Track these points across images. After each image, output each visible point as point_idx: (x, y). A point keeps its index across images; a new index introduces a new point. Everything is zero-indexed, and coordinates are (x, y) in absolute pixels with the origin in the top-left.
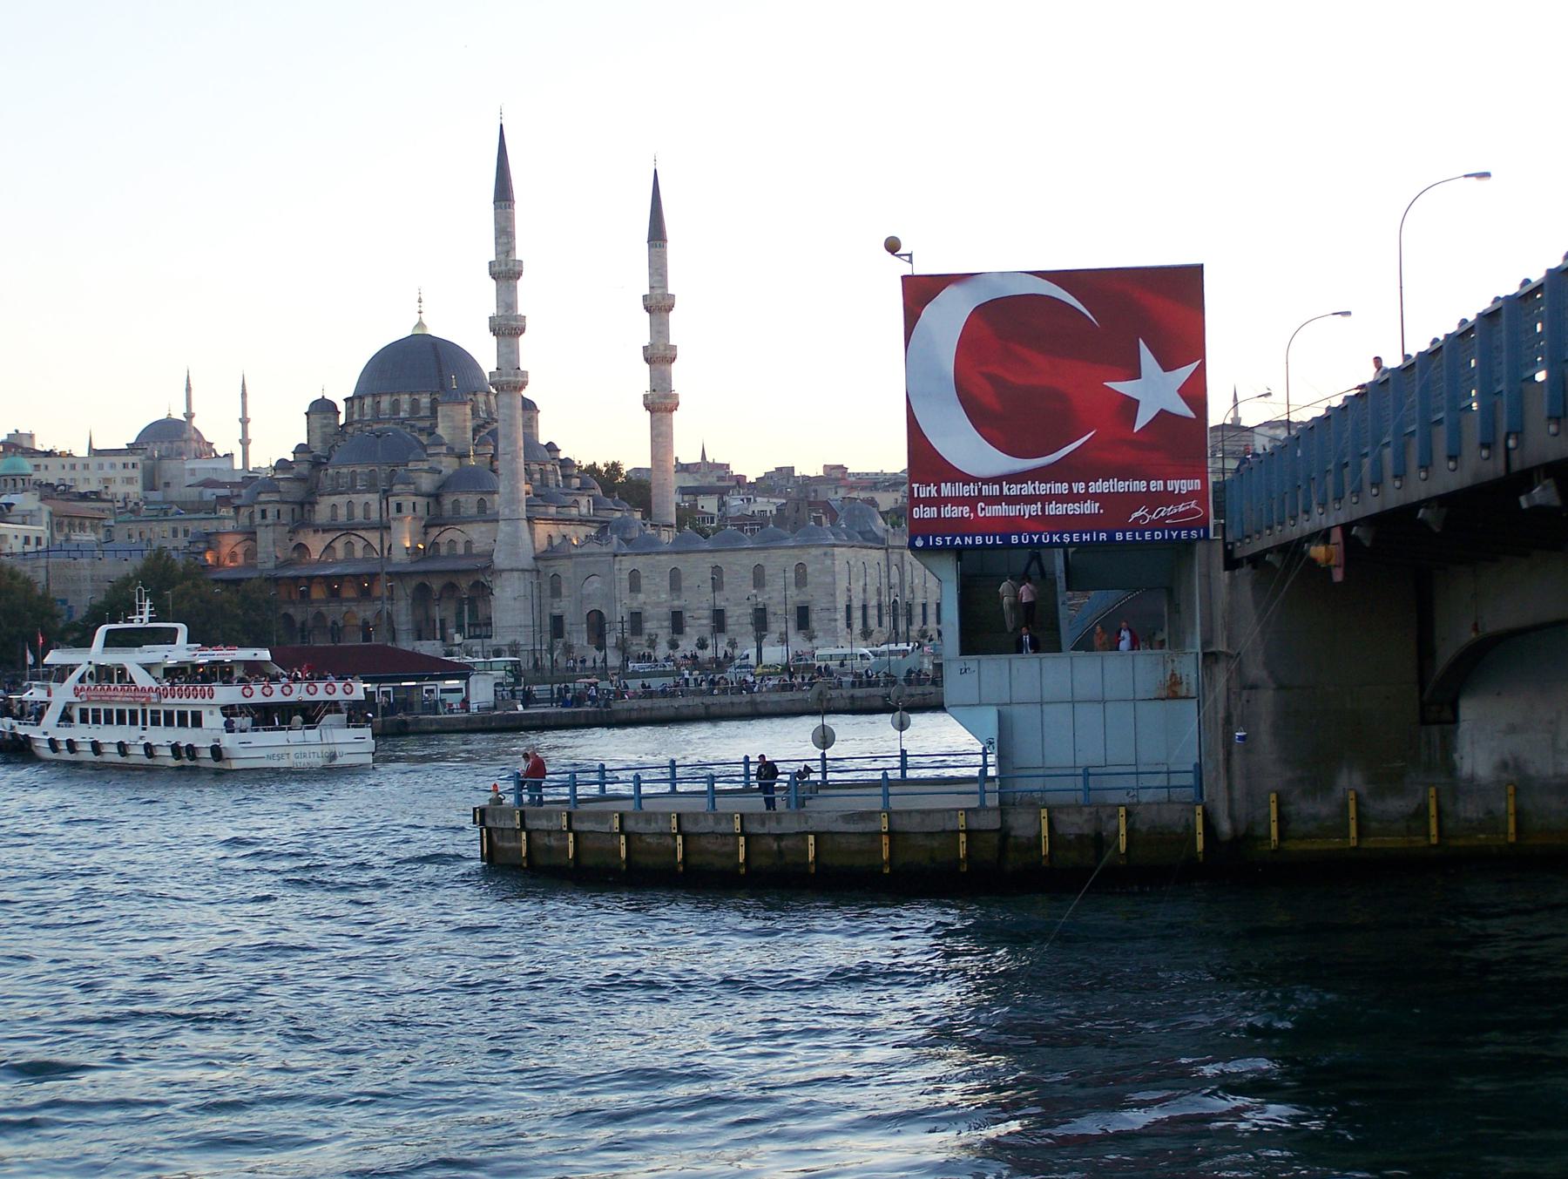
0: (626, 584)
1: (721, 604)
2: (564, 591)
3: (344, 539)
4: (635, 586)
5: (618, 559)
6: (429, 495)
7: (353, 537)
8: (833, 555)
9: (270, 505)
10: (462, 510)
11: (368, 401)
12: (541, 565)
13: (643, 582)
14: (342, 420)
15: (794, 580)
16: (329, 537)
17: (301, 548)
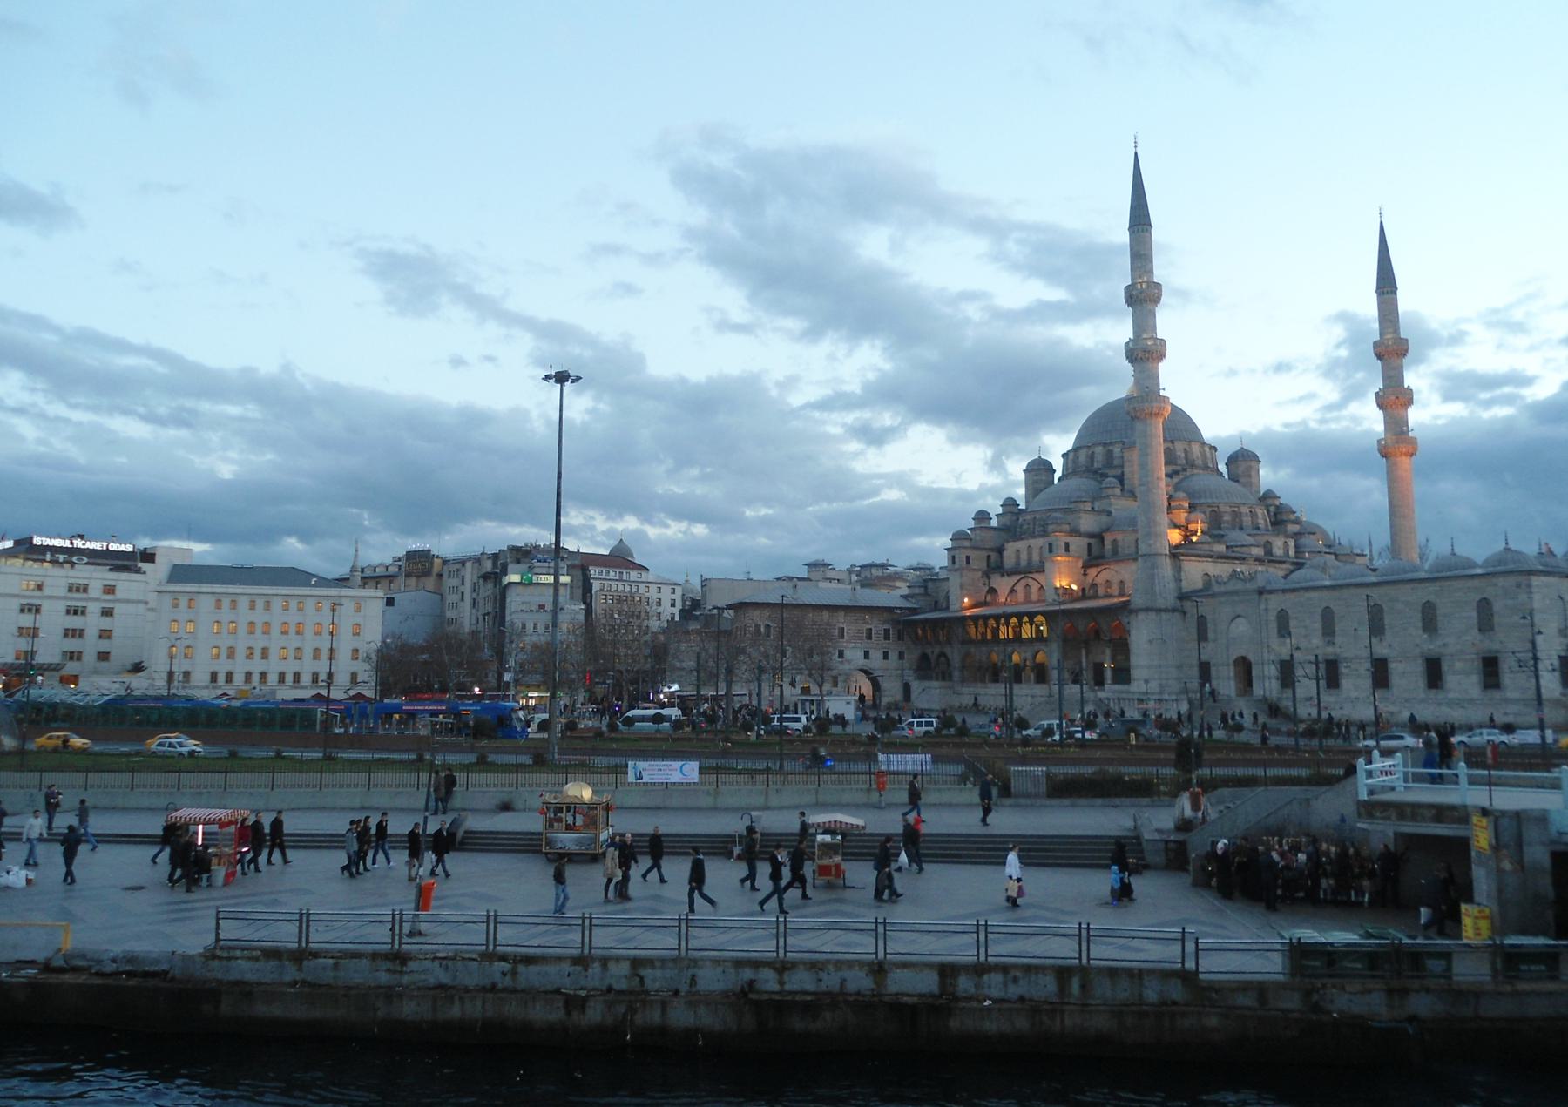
0: (1273, 627)
1: (1381, 650)
2: (1211, 635)
3: (1023, 581)
4: (1284, 630)
5: (1265, 596)
6: (1090, 535)
7: (1030, 580)
8: (1529, 586)
9: (958, 552)
10: (1120, 550)
11: (1071, 456)
12: (1188, 605)
13: (1292, 623)
14: (1058, 475)
15: (1475, 621)
16: (1016, 578)
17: (992, 591)
